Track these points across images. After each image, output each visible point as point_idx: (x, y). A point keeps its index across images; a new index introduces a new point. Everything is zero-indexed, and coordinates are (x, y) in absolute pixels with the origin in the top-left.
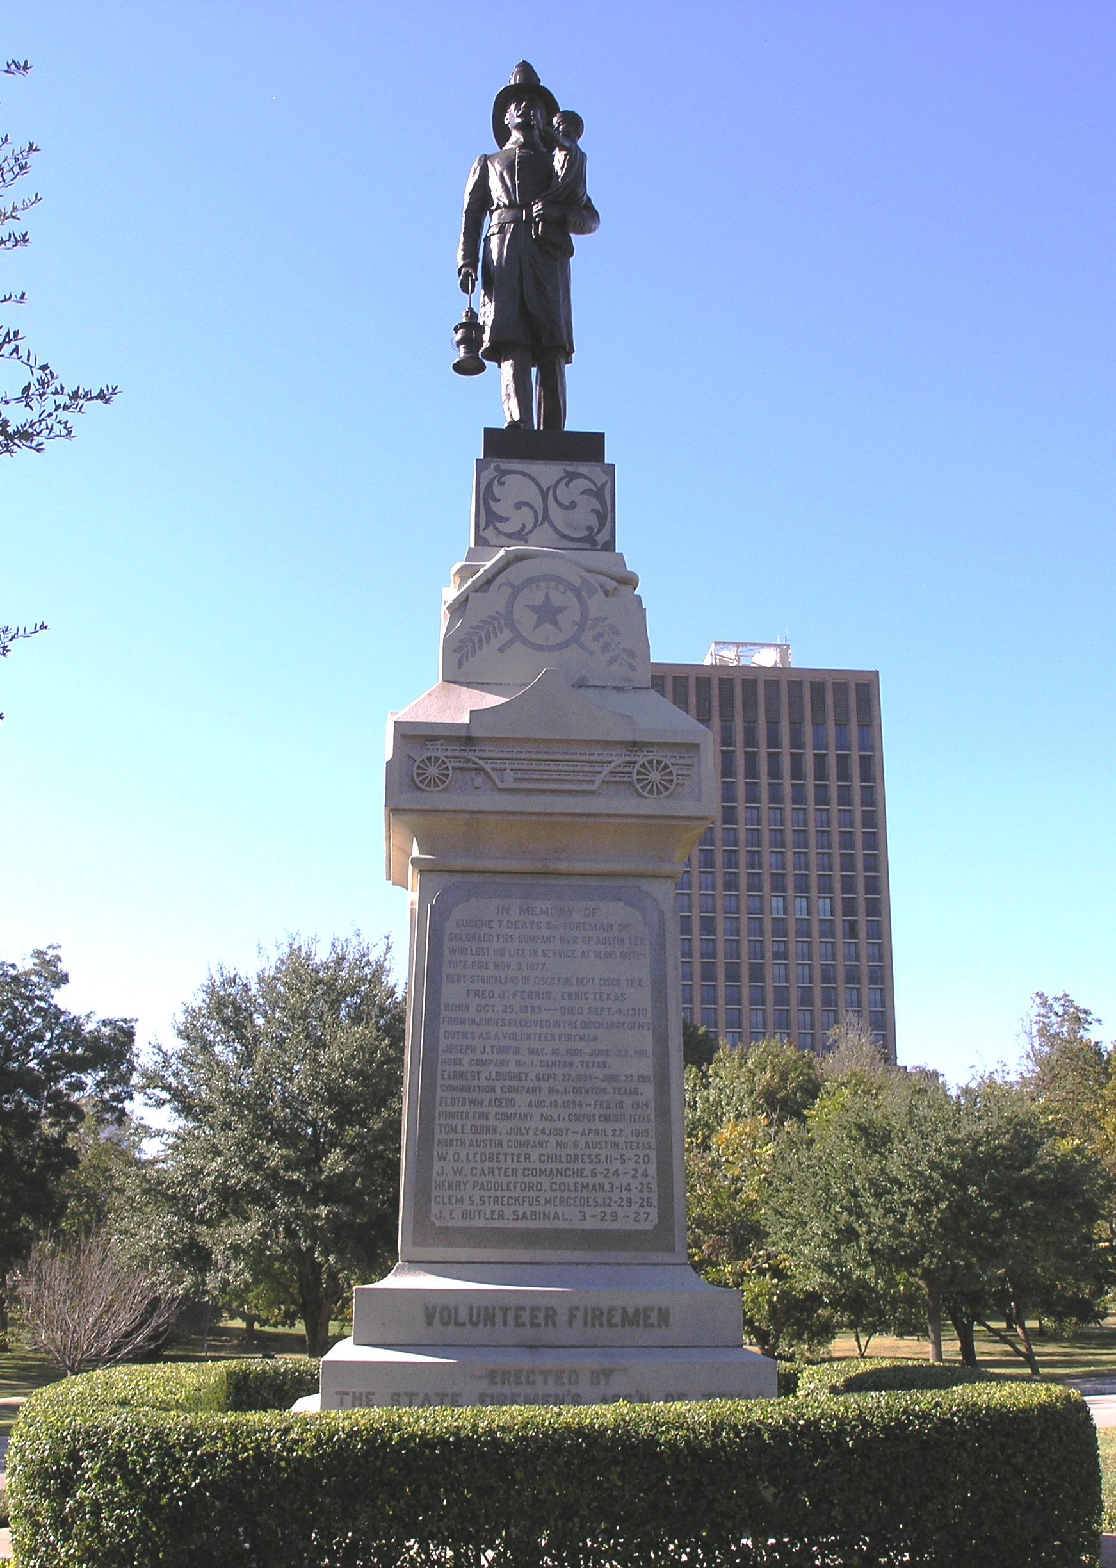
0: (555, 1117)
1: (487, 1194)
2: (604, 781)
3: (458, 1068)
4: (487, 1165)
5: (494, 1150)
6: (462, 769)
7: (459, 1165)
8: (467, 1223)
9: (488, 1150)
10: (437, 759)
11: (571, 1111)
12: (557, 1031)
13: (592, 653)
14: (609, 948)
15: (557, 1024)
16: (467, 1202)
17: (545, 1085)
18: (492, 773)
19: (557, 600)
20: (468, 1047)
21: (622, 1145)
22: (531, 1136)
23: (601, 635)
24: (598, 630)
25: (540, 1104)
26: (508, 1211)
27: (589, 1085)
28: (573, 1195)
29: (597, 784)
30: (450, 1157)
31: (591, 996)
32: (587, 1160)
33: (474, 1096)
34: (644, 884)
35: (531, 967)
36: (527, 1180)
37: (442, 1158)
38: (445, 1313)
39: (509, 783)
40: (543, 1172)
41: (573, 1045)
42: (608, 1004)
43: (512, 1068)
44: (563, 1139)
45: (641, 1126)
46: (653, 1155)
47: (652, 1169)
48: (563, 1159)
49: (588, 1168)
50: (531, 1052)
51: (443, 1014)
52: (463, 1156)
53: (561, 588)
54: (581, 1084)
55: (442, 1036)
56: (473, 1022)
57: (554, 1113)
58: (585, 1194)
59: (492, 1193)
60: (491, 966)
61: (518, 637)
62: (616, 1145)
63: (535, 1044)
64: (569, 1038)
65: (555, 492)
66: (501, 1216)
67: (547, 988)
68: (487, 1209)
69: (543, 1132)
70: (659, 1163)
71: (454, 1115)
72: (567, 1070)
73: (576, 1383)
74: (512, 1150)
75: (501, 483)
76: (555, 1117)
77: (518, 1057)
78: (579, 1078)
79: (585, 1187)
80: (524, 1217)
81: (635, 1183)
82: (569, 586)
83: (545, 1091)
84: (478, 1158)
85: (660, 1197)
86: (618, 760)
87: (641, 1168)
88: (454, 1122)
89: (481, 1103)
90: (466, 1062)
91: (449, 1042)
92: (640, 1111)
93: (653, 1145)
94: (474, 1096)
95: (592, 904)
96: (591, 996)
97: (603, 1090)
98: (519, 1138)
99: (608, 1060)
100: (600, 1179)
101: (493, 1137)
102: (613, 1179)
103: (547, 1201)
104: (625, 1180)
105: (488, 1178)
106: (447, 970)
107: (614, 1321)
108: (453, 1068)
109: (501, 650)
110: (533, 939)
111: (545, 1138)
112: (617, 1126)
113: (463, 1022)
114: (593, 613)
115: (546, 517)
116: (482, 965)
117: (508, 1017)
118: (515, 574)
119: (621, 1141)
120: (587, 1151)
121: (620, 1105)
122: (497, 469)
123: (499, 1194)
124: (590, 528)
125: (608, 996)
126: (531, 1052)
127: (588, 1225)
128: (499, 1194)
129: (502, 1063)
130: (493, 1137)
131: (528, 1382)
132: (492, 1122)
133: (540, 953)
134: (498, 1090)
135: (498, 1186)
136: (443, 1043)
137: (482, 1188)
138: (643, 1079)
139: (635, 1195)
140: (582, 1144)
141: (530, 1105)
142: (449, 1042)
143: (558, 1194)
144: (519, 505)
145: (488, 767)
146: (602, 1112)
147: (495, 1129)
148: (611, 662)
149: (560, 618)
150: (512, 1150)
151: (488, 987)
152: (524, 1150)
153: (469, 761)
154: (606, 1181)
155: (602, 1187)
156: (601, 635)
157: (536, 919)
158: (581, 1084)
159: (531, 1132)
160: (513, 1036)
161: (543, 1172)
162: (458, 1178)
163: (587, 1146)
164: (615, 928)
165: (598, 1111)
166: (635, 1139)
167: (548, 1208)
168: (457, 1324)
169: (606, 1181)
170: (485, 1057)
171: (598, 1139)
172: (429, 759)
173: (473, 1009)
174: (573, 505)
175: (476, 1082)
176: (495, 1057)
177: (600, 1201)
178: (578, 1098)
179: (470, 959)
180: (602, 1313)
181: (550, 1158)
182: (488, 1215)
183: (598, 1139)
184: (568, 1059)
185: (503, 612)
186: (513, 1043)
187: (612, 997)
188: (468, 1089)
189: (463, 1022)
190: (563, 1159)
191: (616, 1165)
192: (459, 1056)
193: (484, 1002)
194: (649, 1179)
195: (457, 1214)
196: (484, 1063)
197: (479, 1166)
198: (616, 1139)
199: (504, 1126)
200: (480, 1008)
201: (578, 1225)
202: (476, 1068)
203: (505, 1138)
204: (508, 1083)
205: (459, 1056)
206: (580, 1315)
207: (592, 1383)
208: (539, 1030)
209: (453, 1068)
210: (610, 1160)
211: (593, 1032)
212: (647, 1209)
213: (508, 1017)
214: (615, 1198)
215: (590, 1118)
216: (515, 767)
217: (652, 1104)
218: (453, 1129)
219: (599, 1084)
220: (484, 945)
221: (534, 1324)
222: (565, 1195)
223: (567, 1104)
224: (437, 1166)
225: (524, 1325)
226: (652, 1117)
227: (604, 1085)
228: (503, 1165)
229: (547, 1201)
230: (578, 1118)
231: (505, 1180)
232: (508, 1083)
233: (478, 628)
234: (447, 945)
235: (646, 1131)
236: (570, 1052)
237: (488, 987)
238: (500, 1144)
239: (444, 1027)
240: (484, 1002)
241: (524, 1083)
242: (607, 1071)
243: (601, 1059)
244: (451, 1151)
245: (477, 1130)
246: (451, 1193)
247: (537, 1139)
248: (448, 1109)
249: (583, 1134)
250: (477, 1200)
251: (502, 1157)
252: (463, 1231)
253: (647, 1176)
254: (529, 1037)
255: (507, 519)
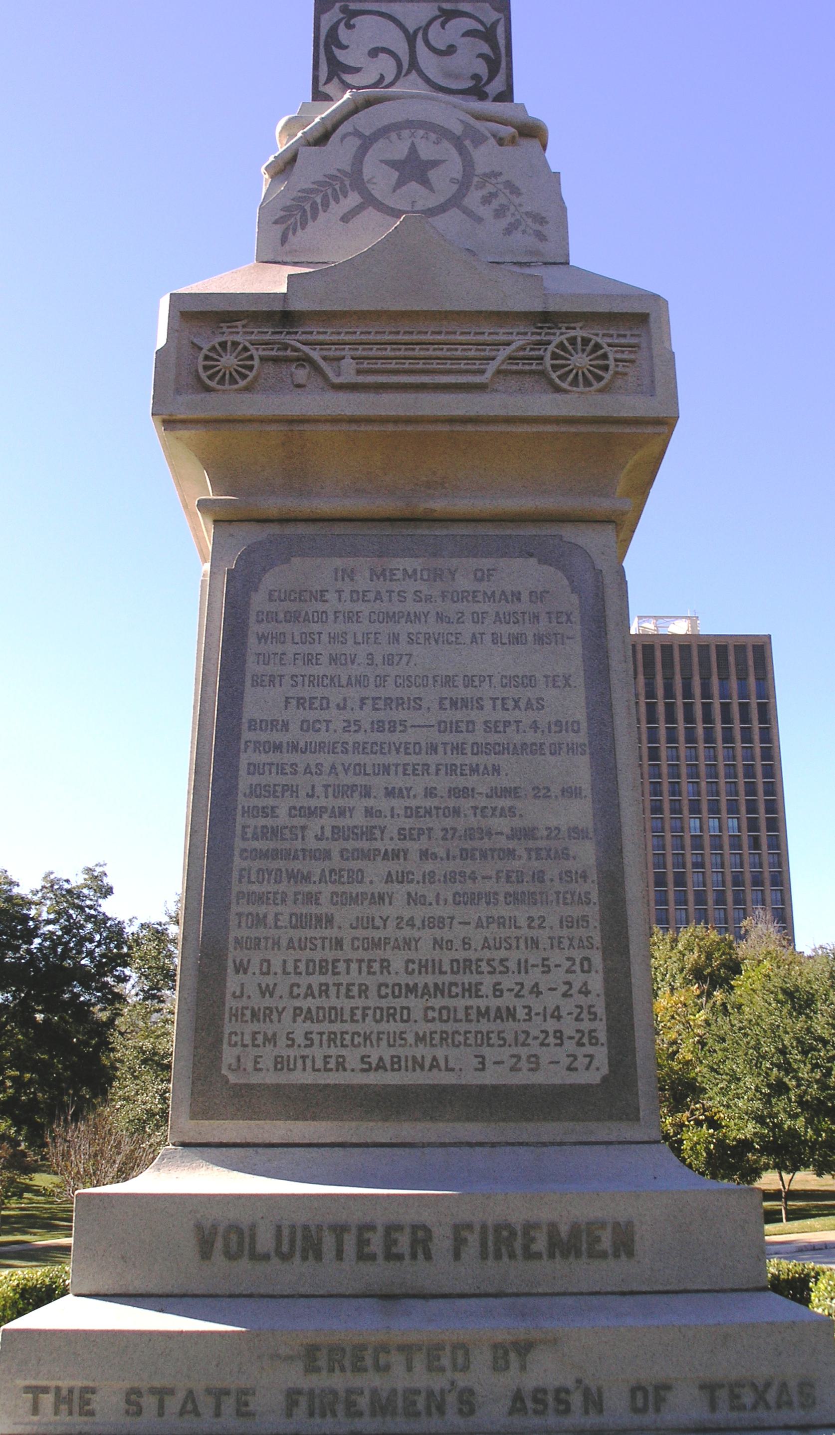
0: (431, 898)
1: (316, 1027)
2: (499, 372)
3: (269, 822)
4: (316, 980)
5: (330, 955)
6: (275, 360)
7: (269, 980)
8: (283, 1078)
9: (317, 956)
10: (235, 344)
11: (458, 887)
12: (432, 760)
13: (480, 220)
14: (515, 629)
15: (433, 749)
16: (282, 1041)
17: (414, 847)
18: (322, 364)
19: (426, 151)
20: (286, 788)
21: (544, 943)
22: (391, 931)
23: (493, 195)
24: (490, 188)
25: (403, 878)
26: (352, 1057)
27: (486, 844)
28: (463, 1027)
29: (488, 375)
30: (255, 968)
31: (488, 704)
32: (485, 967)
33: (296, 865)
34: (569, 532)
35: (389, 660)
36: (384, 1003)
37: (241, 968)
38: (234, 1237)
39: (348, 372)
40: (411, 989)
41: (461, 782)
42: (517, 715)
43: (358, 819)
44: (445, 934)
45: (575, 911)
46: (597, 959)
47: (596, 982)
48: (446, 967)
49: (488, 982)
50: (390, 793)
51: (246, 735)
52: (277, 966)
53: (433, 136)
54: (477, 844)
55: (243, 772)
56: (294, 747)
57: (429, 890)
58: (484, 1026)
59: (326, 1027)
60: (324, 659)
61: (370, 201)
62: (535, 943)
63: (397, 781)
64: (452, 769)
65: (425, 35)
66: (341, 1065)
67: (415, 692)
68: (318, 1052)
69: (411, 923)
70: (607, 971)
71: (261, 899)
72: (449, 822)
73: (466, 1368)
74: (361, 954)
75: (350, 27)
76: (431, 898)
77: (370, 802)
78: (470, 833)
79: (483, 1014)
80: (381, 1066)
81: (567, 1006)
82: (444, 133)
83: (414, 856)
84: (302, 967)
85: (610, 1029)
86: (519, 341)
87: (578, 980)
88: (262, 910)
89: (307, 878)
90: (283, 811)
91: (255, 779)
92: (573, 886)
93: (597, 940)
94: (296, 865)
95: (486, 563)
96: (488, 704)
97: (511, 854)
98: (371, 933)
99: (518, 804)
100: (508, 1000)
101: (327, 933)
102: (531, 1000)
103: (420, 1039)
104: (551, 1000)
105: (318, 1002)
106: (252, 666)
107: (535, 1248)
108: (262, 822)
109: (345, 219)
110: (391, 617)
111: (416, 934)
112: (535, 912)
113: (278, 747)
114: (481, 167)
115: (414, 64)
116: (311, 659)
117: (351, 738)
118: (365, 121)
119: (543, 935)
120: (487, 954)
121: (539, 876)
122: (344, 10)
123: (337, 1027)
124: (476, 77)
125: (516, 702)
126: (390, 793)
127: (489, 1078)
128: (337, 1027)
129: (342, 813)
130: (327, 933)
131: (378, 1368)
132: (325, 908)
133: (403, 638)
134: (335, 855)
135: (335, 1015)
136: (245, 781)
137: (309, 1017)
138: (577, 833)
139: (569, 1027)
140: (477, 942)
141: (389, 879)
142: (255, 779)
143: (439, 1026)
144: (374, 53)
145: (315, 355)
146: (510, 888)
147: (330, 920)
148: (508, 231)
149: (432, 175)
150: (361, 954)
151: (319, 692)
152: (378, 954)
153: (285, 347)
154: (519, 1003)
155: (511, 1014)
156: (493, 195)
157: (396, 587)
158: (477, 844)
159: (391, 924)
160: (360, 770)
161: (411, 989)
162: (268, 1002)
163: (486, 946)
164: (525, 597)
165: (504, 887)
166: (565, 932)
167: (421, 1051)
168: (255, 1256)
169: (519, 1003)
170: (313, 803)
171: (503, 933)
172: (223, 345)
173: (294, 727)
174: (451, 50)
175: (299, 845)
176: (330, 802)
177: (510, 1037)
178: (469, 867)
179: (290, 649)
180: (513, 1233)
181: (423, 966)
182: (319, 1064)
183: (503, 933)
184: (452, 803)
185: (348, 169)
186: (360, 780)
187: (522, 704)
188: (288, 855)
189: (278, 747)
190: (446, 967)
191: (536, 975)
192: (270, 802)
193: (312, 715)
194: (591, 999)
195: (267, 1062)
196: (312, 813)
197: (304, 981)
198: (534, 933)
199: (345, 915)
200: (306, 726)
201: (472, 1078)
202: (299, 821)
203: (347, 935)
204: (351, 845)
205: (270, 802)
206: (473, 1239)
207: (495, 1368)
208: (404, 759)
209: (262, 822)
210: (523, 967)
211: (492, 759)
212: (589, 1049)
213: (351, 738)
214: (534, 1032)
215: (490, 898)
216: (359, 353)
217: (594, 876)
218: (261, 921)
219: (502, 842)
220: (316, 627)
221: (392, 1256)
222: (449, 1027)
223: (451, 878)
224: (233, 983)
225: (373, 1257)
226: (594, 897)
227: (511, 845)
228: (344, 979)
229: (420, 1039)
230: (473, 899)
231: (348, 1004)
232: (351, 845)
233: (311, 191)
234: (254, 628)
235: (585, 918)
236: (454, 792)
237: (319, 692)
238: (339, 943)
239: (245, 758)
240: (312, 715)
241: (378, 844)
242: (517, 823)
243: (506, 803)
244: (256, 958)
245: (300, 921)
246: (255, 1027)
247: (401, 934)
248: (255, 888)
249: (479, 925)
250: (300, 1040)
251: (342, 967)
252: (277, 1090)
253: (587, 993)
254: (386, 769)
255: (357, 70)
